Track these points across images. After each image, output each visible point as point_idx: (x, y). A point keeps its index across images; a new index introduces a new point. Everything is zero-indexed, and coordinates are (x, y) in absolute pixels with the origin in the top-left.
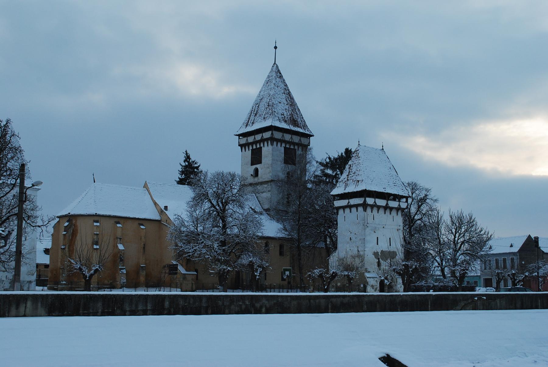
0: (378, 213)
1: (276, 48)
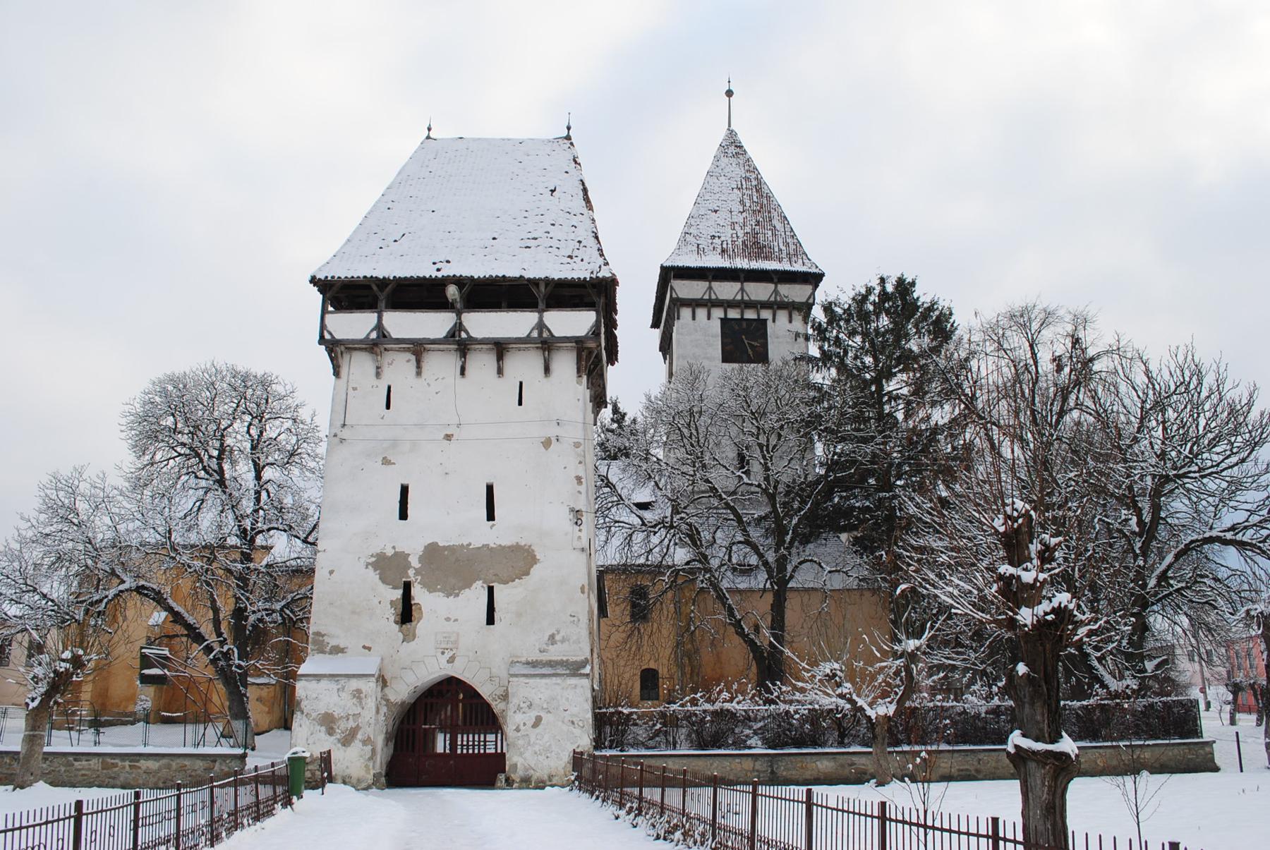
0: (419, 373)
1: (729, 93)
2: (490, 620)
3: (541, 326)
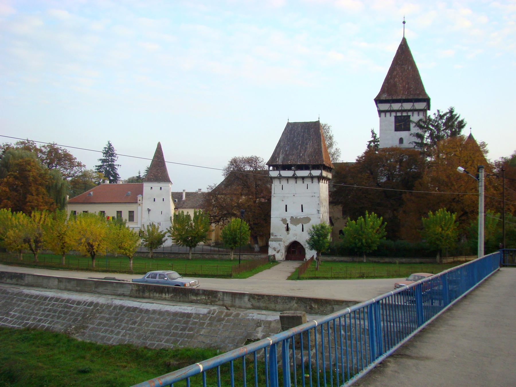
0: (288, 183)
1: (404, 23)
2: (303, 231)
3: (310, 173)
